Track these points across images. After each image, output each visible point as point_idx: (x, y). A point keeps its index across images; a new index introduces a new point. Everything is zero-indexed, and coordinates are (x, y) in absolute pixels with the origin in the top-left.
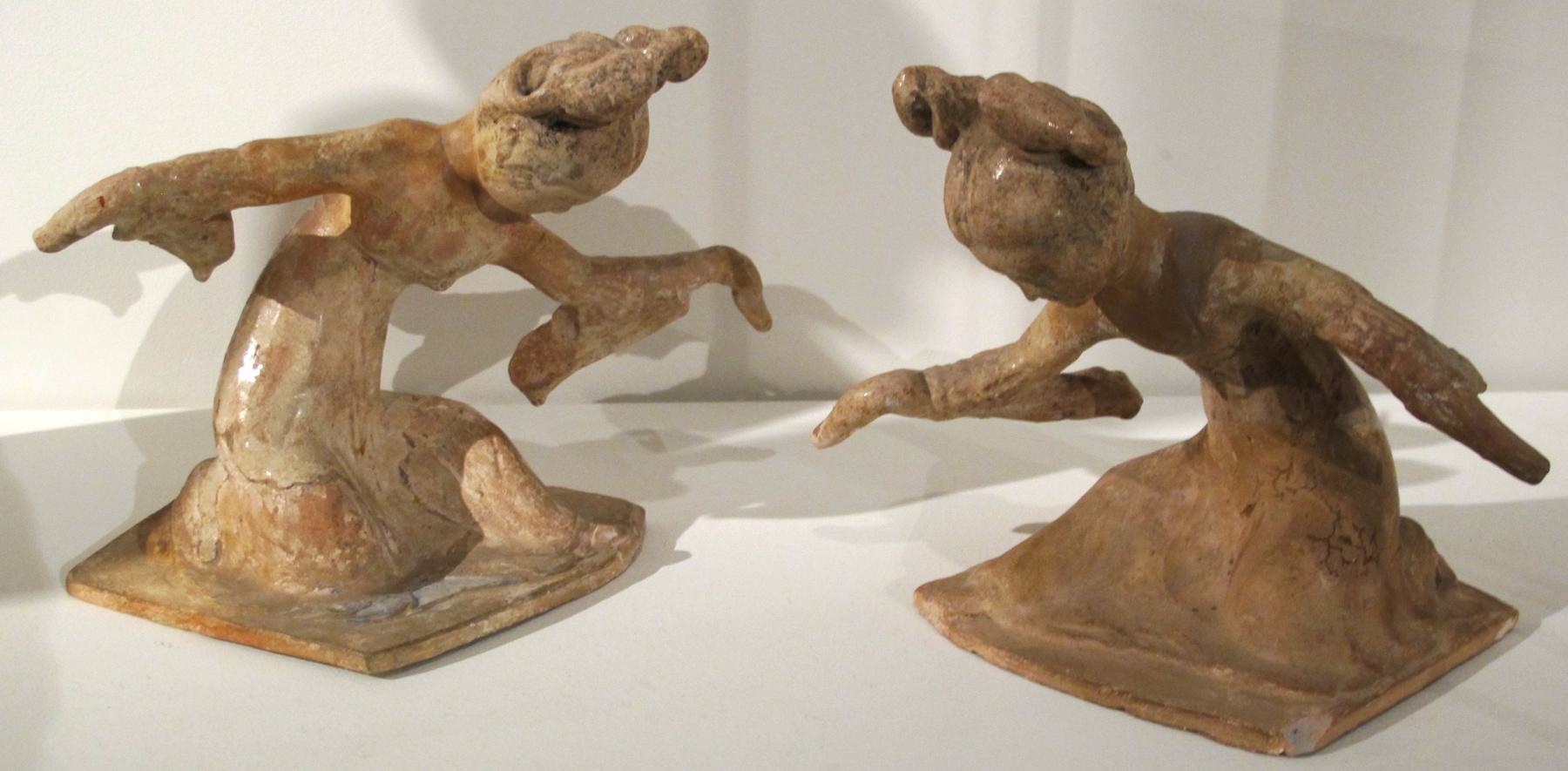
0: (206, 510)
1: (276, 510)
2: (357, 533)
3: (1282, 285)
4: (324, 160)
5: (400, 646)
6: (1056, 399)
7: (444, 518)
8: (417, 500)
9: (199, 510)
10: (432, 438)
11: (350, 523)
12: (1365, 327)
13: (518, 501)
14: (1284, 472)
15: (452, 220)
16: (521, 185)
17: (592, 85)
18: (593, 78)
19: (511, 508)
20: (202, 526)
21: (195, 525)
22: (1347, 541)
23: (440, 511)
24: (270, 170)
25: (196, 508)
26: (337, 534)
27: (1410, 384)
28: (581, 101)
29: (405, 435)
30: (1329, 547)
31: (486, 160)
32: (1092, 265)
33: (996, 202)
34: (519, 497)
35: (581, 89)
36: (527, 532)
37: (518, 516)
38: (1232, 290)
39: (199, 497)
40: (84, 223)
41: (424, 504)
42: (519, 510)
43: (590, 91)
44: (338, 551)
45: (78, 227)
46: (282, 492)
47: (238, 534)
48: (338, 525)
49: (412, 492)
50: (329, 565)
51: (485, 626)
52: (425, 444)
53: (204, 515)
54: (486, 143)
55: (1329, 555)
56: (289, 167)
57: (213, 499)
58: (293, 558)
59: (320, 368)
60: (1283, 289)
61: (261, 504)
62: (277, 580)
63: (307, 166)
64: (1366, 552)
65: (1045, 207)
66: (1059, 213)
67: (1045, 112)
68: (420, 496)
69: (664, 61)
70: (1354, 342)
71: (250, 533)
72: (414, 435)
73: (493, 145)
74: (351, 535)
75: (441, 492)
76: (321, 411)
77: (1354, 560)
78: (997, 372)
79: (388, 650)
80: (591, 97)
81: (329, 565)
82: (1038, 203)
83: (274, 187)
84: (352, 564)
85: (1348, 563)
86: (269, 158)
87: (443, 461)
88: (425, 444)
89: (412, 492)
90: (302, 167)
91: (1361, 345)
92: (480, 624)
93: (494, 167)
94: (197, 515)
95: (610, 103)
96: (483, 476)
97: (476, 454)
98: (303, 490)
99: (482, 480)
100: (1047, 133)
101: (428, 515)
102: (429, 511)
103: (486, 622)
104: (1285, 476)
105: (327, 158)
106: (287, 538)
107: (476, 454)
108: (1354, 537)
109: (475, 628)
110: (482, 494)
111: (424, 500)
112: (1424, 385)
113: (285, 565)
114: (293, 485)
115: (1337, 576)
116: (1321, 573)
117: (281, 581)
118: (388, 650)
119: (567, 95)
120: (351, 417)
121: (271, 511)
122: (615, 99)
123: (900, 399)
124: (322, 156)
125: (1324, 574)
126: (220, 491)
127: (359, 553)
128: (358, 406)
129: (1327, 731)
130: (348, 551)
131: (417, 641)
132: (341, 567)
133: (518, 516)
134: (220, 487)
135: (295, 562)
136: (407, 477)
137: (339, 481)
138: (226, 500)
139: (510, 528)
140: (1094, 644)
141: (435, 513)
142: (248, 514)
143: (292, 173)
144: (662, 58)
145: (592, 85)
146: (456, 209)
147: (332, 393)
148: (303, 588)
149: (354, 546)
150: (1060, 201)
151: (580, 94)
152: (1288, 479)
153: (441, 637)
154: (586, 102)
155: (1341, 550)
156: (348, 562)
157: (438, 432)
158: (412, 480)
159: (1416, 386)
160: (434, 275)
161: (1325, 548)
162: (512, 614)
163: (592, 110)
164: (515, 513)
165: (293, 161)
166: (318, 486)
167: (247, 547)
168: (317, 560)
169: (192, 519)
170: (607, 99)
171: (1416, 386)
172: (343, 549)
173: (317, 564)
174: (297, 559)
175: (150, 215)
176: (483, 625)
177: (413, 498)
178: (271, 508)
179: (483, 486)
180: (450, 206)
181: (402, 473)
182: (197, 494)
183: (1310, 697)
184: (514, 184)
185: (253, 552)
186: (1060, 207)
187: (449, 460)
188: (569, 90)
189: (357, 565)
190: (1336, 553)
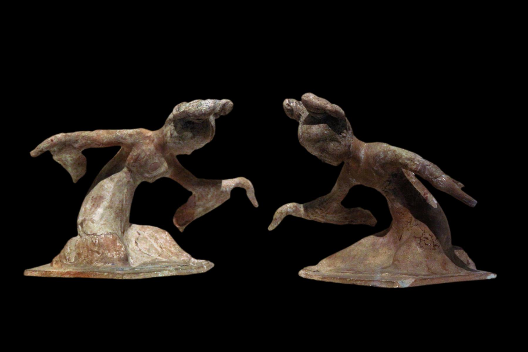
0: (72, 248)
1: (96, 242)
2: (121, 248)
3: (396, 155)
4: (118, 135)
5: (133, 273)
6: (346, 216)
7: (149, 255)
8: (140, 250)
9: (70, 249)
10: (146, 233)
11: (119, 246)
12: (418, 164)
13: (173, 249)
14: (409, 222)
15: (156, 158)
16: (177, 143)
17: (197, 107)
18: (198, 105)
19: (170, 251)
20: (70, 254)
21: (68, 254)
22: (427, 238)
23: (147, 253)
24: (102, 136)
25: (68, 249)
26: (114, 248)
27: (430, 177)
28: (194, 112)
29: (137, 232)
30: (421, 239)
31: (167, 136)
32: (338, 149)
33: (308, 129)
34: (173, 248)
35: (194, 108)
36: (175, 257)
37: (172, 253)
38: (382, 158)
39: (70, 245)
40: (46, 147)
41: (142, 251)
42: (173, 251)
43: (197, 109)
44: (115, 252)
45: (44, 148)
46: (98, 236)
47: (82, 252)
48: (115, 245)
49: (139, 248)
50: (112, 256)
51: (160, 274)
52: (144, 234)
53: (71, 250)
54: (167, 131)
55: (420, 242)
56: (108, 136)
57: (75, 244)
58: (100, 255)
59: (112, 203)
60: (396, 156)
61: (91, 241)
62: (94, 263)
63: (113, 136)
64: (434, 243)
65: (322, 130)
66: (326, 132)
67: (318, 100)
68: (141, 249)
69: (220, 107)
70: (416, 168)
71: (86, 251)
72: (140, 232)
73: (169, 132)
74: (119, 248)
75: (148, 248)
76: (112, 216)
77: (429, 244)
78: (322, 200)
79: (129, 274)
80: (197, 110)
81: (112, 256)
82: (320, 129)
83: (103, 141)
84: (118, 256)
85: (427, 245)
86: (102, 133)
87: (149, 239)
88: (144, 234)
89: (139, 248)
90: (111, 136)
91: (417, 169)
92: (158, 273)
93: (169, 139)
94: (69, 250)
95: (202, 112)
96: (162, 242)
97: (160, 236)
98: (105, 235)
99: (161, 244)
100: (319, 106)
101: (143, 254)
102: (145, 253)
103: (160, 273)
104: (409, 223)
105: (119, 134)
106: (99, 249)
107: (160, 236)
108: (430, 238)
109: (157, 274)
110: (161, 248)
111: (142, 250)
112: (434, 176)
113: (97, 257)
114: (102, 234)
115: (423, 248)
116: (418, 247)
117: (96, 263)
118: (129, 274)
119: (190, 110)
120: (121, 221)
121: (94, 242)
122: (204, 111)
123: (292, 209)
124: (118, 134)
125: (419, 247)
126: (77, 242)
127: (121, 254)
128: (123, 218)
129: (413, 282)
130: (118, 253)
131: (138, 273)
132: (115, 257)
133: (172, 253)
134: (77, 241)
135: (101, 256)
136: (137, 243)
137: (116, 235)
138: (79, 244)
139: (170, 256)
140: (349, 274)
141: (146, 254)
142: (87, 245)
143: (109, 138)
144: (220, 106)
145: (197, 107)
146: (157, 155)
147: (115, 211)
148: (103, 264)
149: (120, 252)
150: (326, 128)
151: (194, 110)
152: (410, 224)
153: (145, 273)
154: (196, 112)
155: (425, 241)
156: (118, 256)
157: (148, 231)
158: (139, 244)
159: (432, 177)
160: (149, 177)
161: (419, 240)
162: (168, 273)
163: (197, 114)
164: (172, 252)
165: (109, 134)
166: (110, 235)
167: (85, 255)
168: (108, 255)
169: (67, 252)
170: (201, 111)
171: (432, 177)
172: (116, 252)
173: (108, 256)
174: (102, 255)
175: (66, 146)
176: (159, 274)
177: (139, 249)
178: (94, 241)
179: (162, 246)
180: (155, 154)
181: (136, 242)
182: (69, 245)
183: (410, 276)
184: (175, 143)
185: (87, 256)
186: (326, 130)
187: (151, 239)
188: (191, 109)
189: (120, 257)
190: (423, 242)
